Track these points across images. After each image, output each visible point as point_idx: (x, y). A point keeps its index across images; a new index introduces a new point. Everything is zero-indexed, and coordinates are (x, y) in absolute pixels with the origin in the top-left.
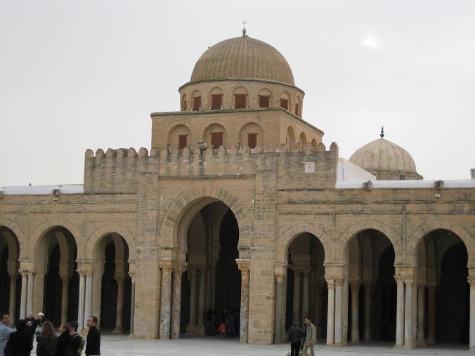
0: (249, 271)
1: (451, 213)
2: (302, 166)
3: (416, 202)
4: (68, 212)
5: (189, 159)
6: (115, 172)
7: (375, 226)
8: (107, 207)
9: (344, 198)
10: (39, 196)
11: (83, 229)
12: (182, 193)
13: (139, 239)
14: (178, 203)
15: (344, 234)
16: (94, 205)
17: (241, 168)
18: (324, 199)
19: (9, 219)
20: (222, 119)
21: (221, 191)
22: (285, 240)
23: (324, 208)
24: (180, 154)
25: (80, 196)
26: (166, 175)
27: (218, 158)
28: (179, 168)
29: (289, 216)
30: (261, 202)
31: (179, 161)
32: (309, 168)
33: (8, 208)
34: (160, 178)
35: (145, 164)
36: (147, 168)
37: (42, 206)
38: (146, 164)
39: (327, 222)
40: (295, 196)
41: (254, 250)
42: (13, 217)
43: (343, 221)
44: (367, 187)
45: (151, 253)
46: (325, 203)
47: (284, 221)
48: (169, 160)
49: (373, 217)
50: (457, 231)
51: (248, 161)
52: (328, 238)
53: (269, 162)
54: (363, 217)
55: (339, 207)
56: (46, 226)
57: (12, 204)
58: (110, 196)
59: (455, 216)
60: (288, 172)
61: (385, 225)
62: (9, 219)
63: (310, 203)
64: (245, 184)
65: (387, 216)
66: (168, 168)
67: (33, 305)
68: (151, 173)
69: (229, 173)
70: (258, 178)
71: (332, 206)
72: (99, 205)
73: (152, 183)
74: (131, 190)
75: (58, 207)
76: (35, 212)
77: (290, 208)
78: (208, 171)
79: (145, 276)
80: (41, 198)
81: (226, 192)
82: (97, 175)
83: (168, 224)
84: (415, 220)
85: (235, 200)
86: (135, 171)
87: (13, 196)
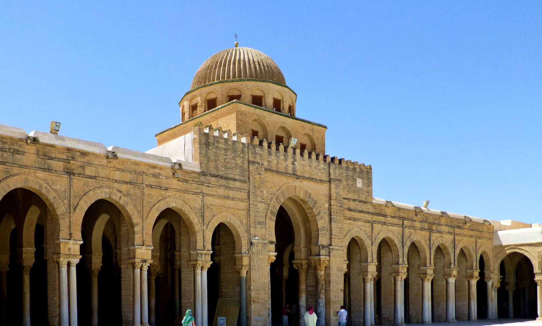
0: (327, 268)
1: (422, 229)
2: (355, 180)
3: (408, 219)
4: (186, 191)
5: (284, 156)
6: (227, 155)
7: (391, 235)
8: (222, 191)
9: (376, 212)
10: (154, 167)
12: (280, 188)
13: (252, 231)
14: (277, 198)
15: (377, 240)
16: (210, 188)
17: (320, 174)
18: (367, 210)
19: (120, 192)
21: (307, 192)
23: (368, 217)
24: (277, 149)
25: (197, 176)
26: (268, 167)
27: (304, 161)
28: (278, 163)
29: (349, 221)
30: (335, 207)
31: (277, 157)
32: (359, 183)
33: (117, 175)
34: (266, 170)
35: (252, 154)
36: (255, 157)
37: (158, 180)
40: (352, 205)
41: (333, 249)
42: (124, 188)
45: (263, 246)
46: (368, 213)
48: (270, 154)
49: (390, 227)
51: (324, 169)
52: (370, 243)
53: (337, 171)
54: (385, 226)
55: (375, 218)
56: (162, 207)
57: (123, 170)
58: (224, 180)
59: (423, 232)
60: (348, 184)
62: (120, 192)
63: (360, 212)
65: (396, 228)
66: (269, 162)
67: (134, 307)
68: (259, 163)
69: (312, 177)
70: (333, 185)
71: (371, 216)
72: (215, 189)
73: (260, 174)
74: (242, 178)
75: (174, 183)
76: (151, 186)
77: (349, 214)
78: (298, 174)
79: (259, 270)
80: (157, 171)
81: (310, 194)
83: (271, 219)
85: (316, 203)
86: (243, 157)
87: (124, 161)
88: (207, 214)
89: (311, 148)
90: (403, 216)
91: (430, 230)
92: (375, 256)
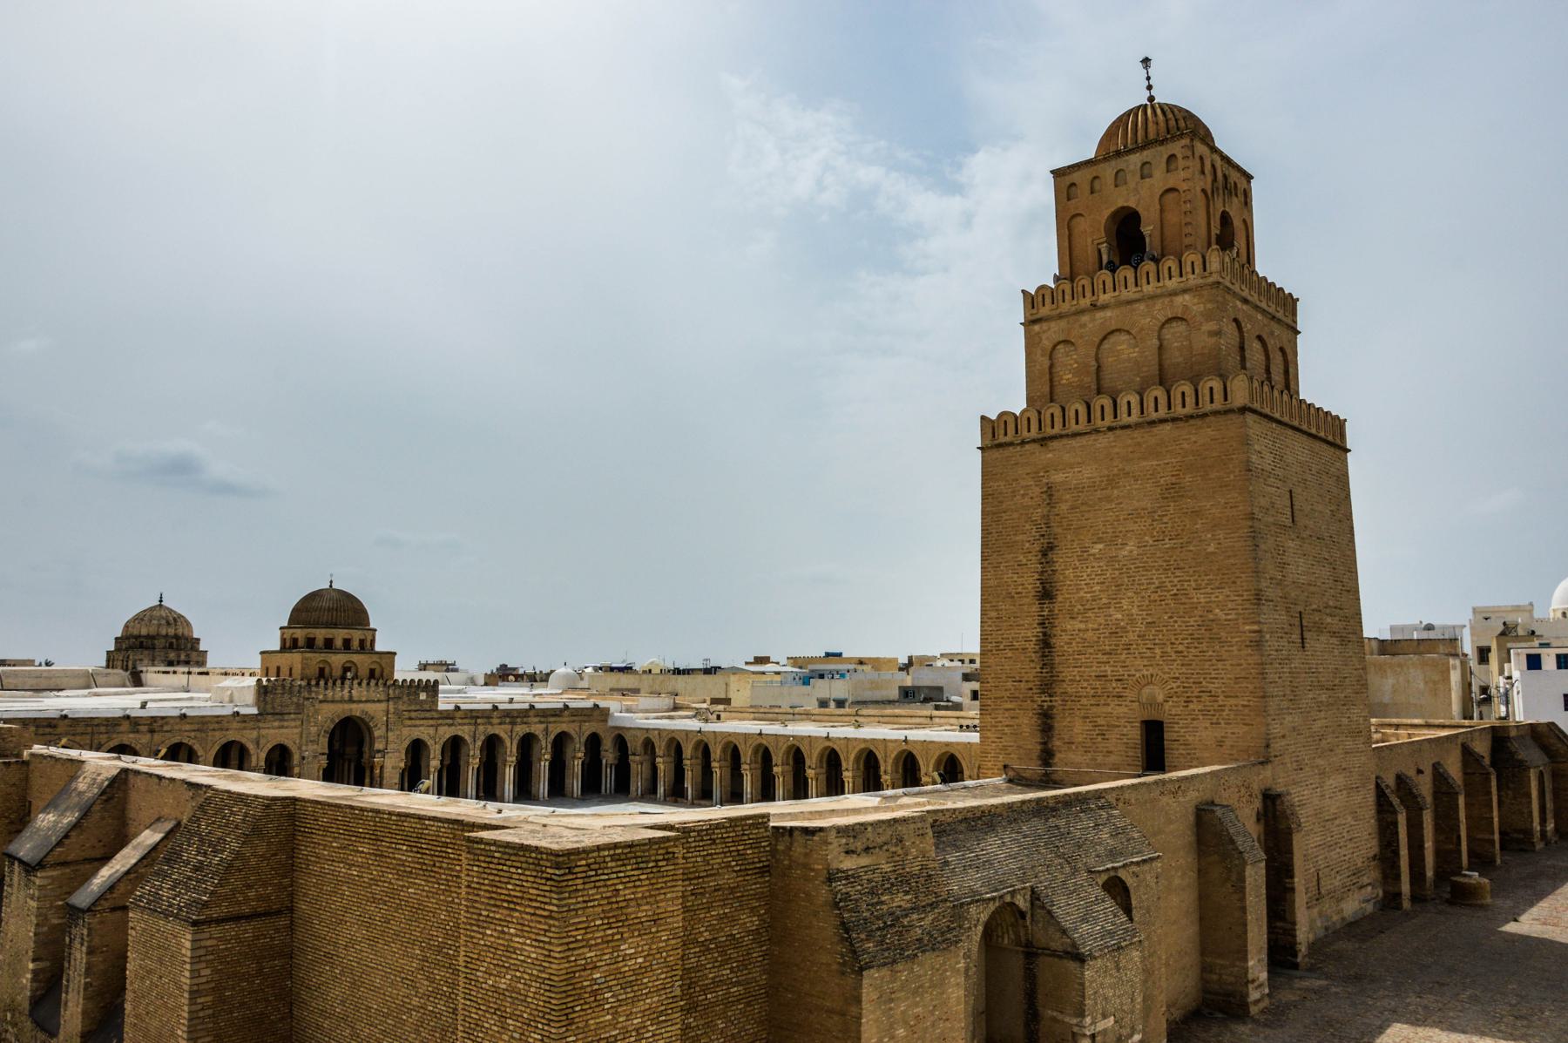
11: (258, 744)
20: (356, 658)
22: (407, 743)
32: (423, 696)
33: (188, 727)
38: (310, 692)
39: (432, 731)
40: (413, 715)
43: (442, 730)
44: (457, 708)
47: (406, 731)
50: (502, 735)
56: (224, 741)
61: (465, 731)
64: (383, 706)
75: (235, 725)
82: (268, 699)
84: (481, 728)
88: (262, 741)
89: (380, 670)
90: (474, 716)
91: (513, 723)
92: (438, 752)
